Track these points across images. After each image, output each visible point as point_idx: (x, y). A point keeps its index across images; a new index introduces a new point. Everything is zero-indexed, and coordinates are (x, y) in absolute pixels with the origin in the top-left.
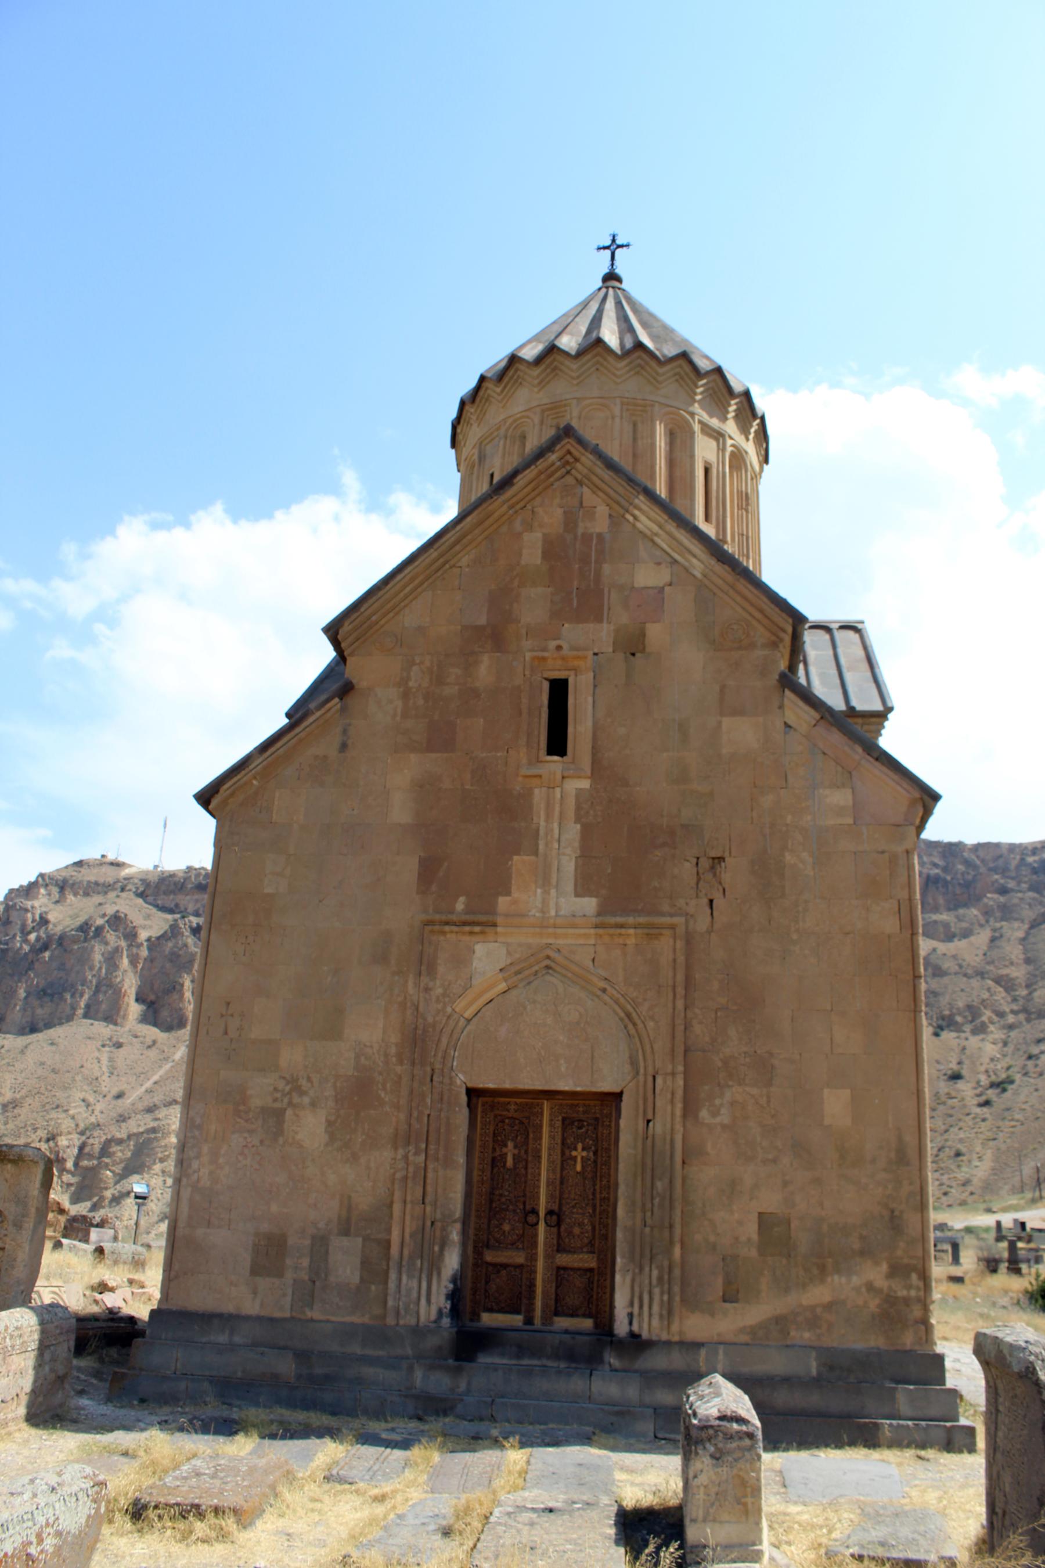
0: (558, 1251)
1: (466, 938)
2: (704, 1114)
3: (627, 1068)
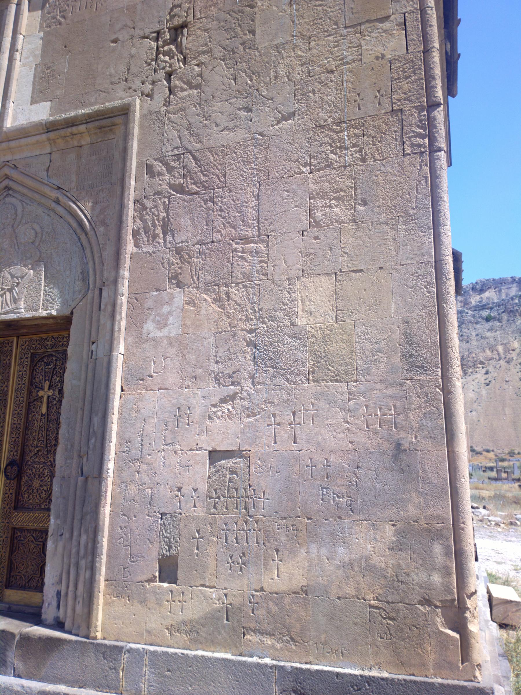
0: (16, 508)
2: (149, 326)
3: (79, 285)
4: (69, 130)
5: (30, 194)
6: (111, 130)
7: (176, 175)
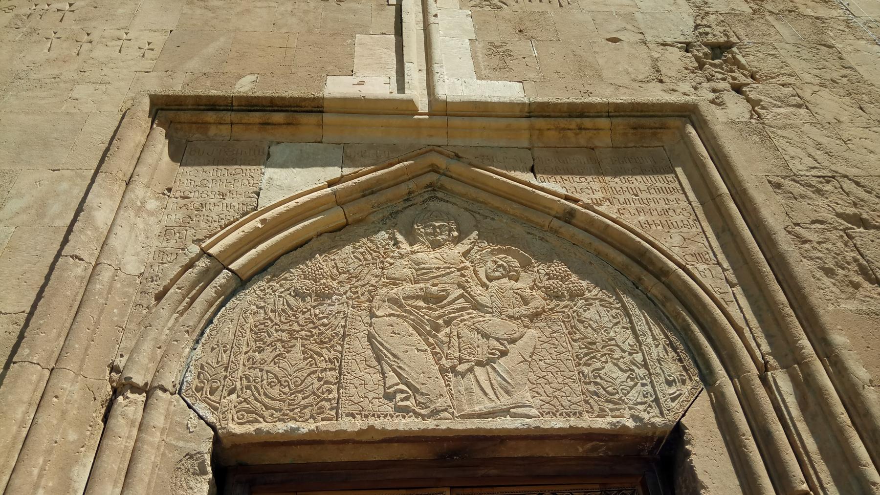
1: (254, 135)
4: (578, 120)
5: (496, 202)
6: (654, 134)
7: (839, 202)
